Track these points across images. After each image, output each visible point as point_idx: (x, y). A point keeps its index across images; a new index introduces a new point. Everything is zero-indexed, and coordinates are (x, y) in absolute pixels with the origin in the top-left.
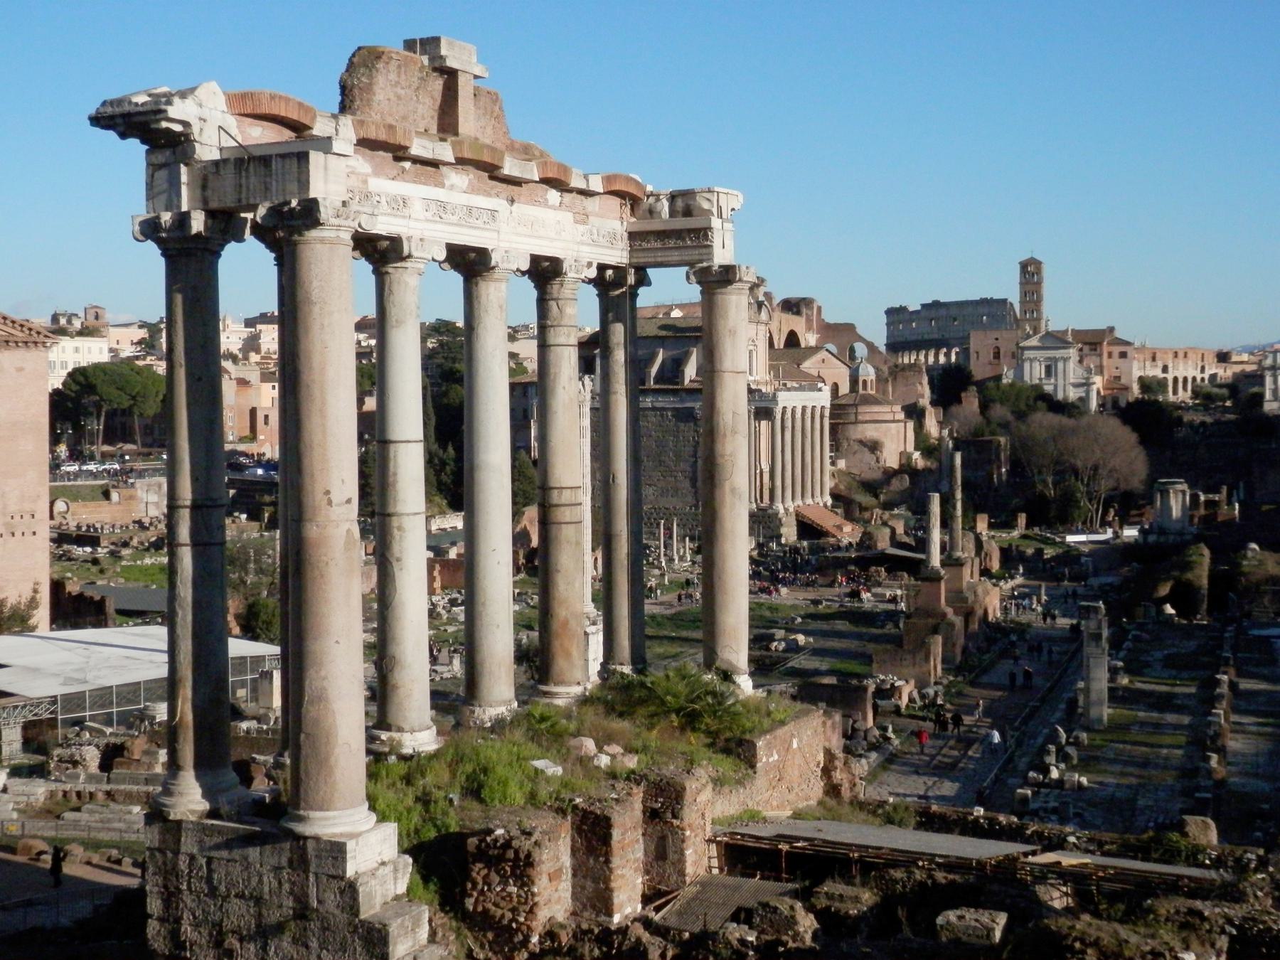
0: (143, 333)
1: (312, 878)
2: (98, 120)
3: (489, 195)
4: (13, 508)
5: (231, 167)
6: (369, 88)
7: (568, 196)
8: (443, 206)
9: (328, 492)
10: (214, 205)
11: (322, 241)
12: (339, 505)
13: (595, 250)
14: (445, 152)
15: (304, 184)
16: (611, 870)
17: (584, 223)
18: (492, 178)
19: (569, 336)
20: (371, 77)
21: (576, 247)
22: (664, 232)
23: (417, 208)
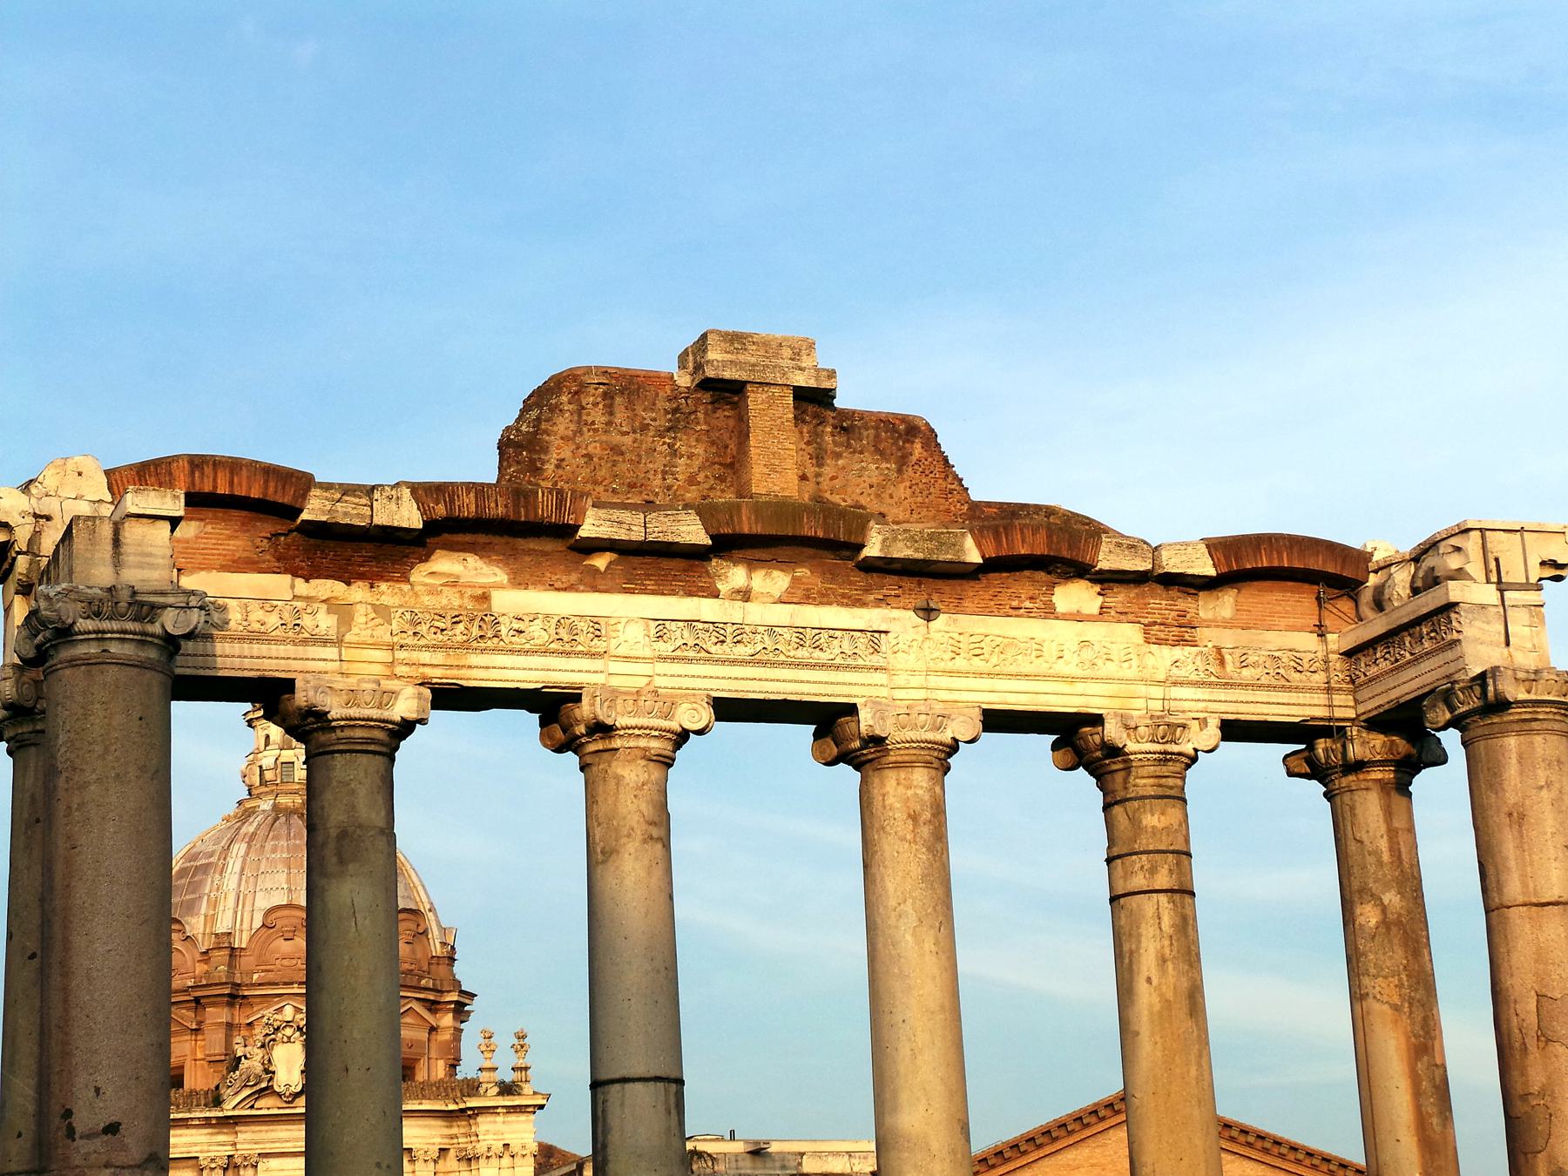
3: (864, 604)
7: (1120, 597)
9: (68, 1114)
11: (73, 663)
12: (89, 1136)
13: (1221, 694)
14: (692, 532)
17: (1180, 641)
19: (1153, 871)
21: (1157, 692)
23: (633, 638)
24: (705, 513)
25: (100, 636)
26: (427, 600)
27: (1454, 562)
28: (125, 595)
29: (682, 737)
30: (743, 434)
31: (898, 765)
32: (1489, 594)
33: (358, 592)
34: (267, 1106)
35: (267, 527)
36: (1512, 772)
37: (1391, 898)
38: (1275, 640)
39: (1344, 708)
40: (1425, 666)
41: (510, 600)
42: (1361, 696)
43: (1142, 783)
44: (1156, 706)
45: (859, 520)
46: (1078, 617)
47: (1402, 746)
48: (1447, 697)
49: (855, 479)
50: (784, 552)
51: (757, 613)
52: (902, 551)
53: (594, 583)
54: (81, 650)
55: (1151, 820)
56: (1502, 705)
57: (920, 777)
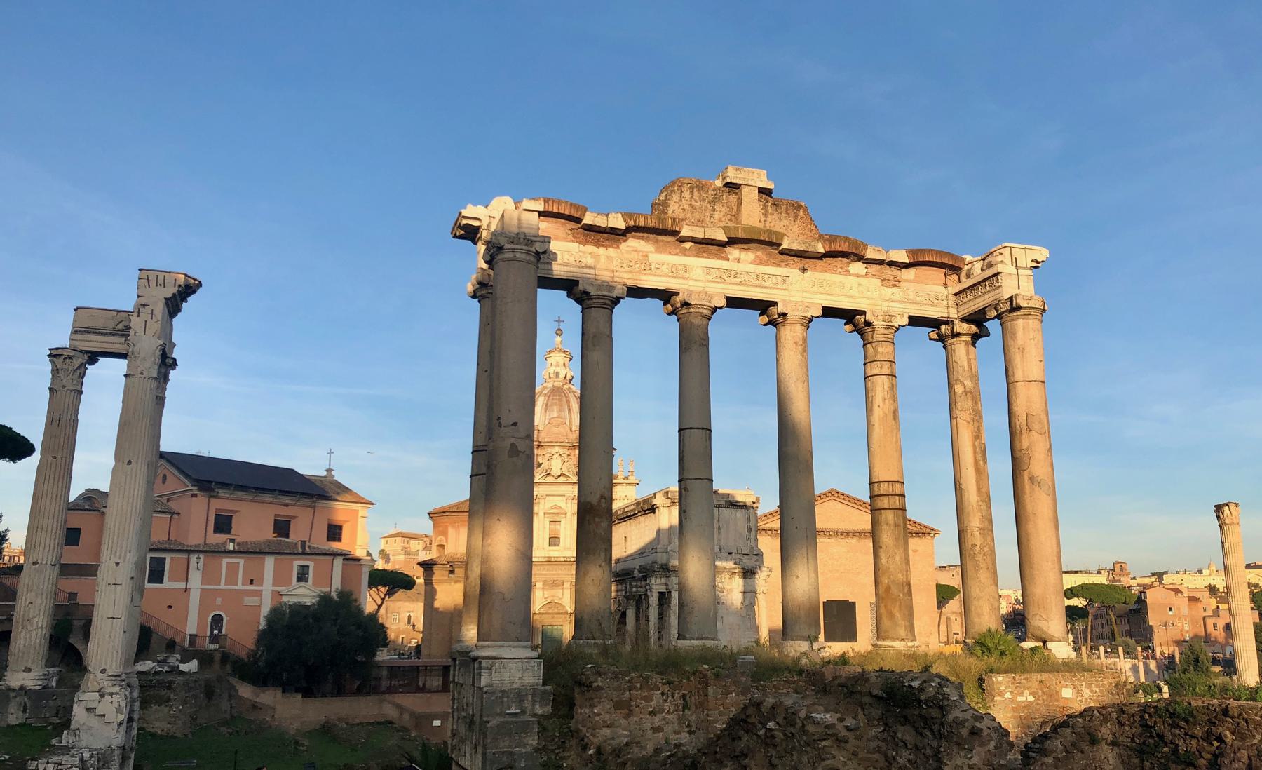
3: (779, 266)
7: (874, 268)
11: (503, 260)
13: (909, 306)
18: (783, 253)
24: (725, 229)
25: (513, 250)
26: (626, 256)
27: (999, 258)
28: (522, 236)
29: (714, 310)
30: (740, 204)
31: (791, 324)
32: (1013, 270)
33: (602, 250)
34: (549, 479)
35: (572, 225)
36: (1020, 334)
37: (968, 383)
38: (928, 288)
39: (953, 314)
40: (987, 296)
41: (656, 258)
42: (961, 308)
43: (879, 336)
44: (885, 309)
45: (782, 236)
46: (858, 276)
47: (974, 329)
48: (996, 307)
49: (778, 223)
50: (753, 246)
51: (742, 267)
52: (795, 247)
53: (685, 253)
54: (506, 255)
55: (880, 349)
56: (1018, 308)
57: (799, 329)
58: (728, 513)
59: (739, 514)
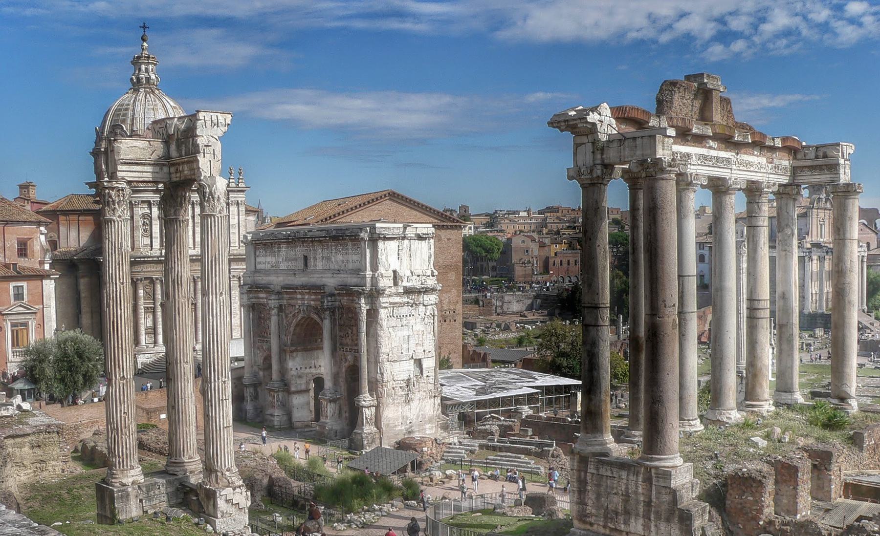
0: (487, 219)
1: (654, 488)
2: (551, 124)
4: (446, 308)
5: (615, 144)
6: (671, 103)
8: (705, 157)
10: (606, 162)
11: (662, 179)
13: (776, 176)
15: (655, 152)
16: (797, 494)
20: (672, 95)
22: (812, 166)
23: (694, 160)
52: (740, 139)
58: (416, 244)
59: (424, 244)
